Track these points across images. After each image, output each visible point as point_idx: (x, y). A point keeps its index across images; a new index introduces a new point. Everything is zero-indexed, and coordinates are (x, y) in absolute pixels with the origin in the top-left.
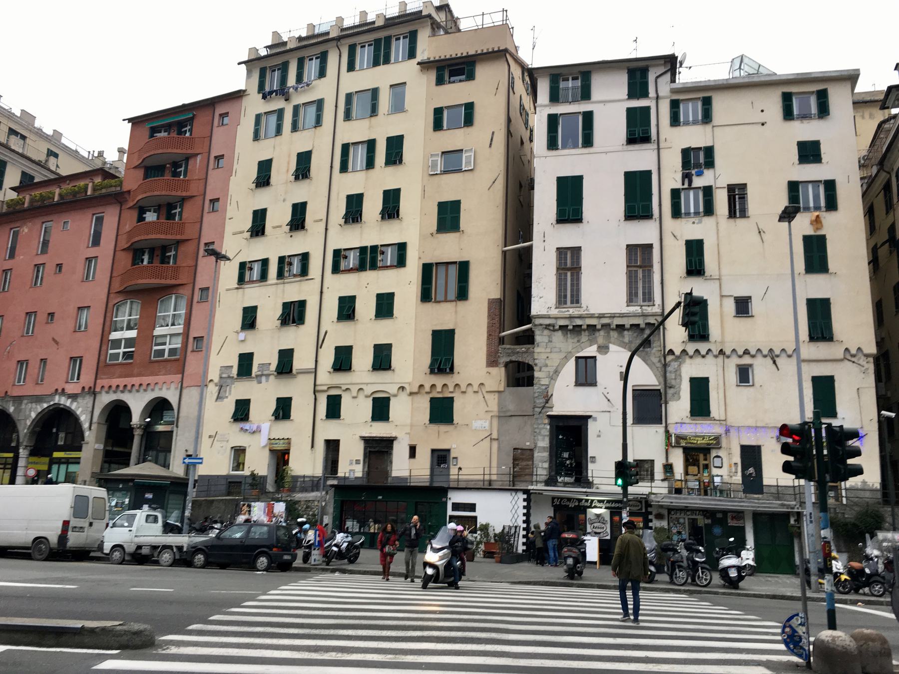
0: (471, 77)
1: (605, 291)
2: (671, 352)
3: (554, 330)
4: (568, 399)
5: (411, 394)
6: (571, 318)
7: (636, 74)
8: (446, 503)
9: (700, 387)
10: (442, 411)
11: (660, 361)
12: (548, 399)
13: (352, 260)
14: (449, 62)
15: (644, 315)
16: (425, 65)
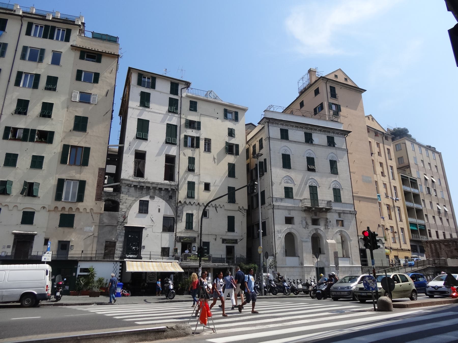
0: (99, 61)
1: (155, 172)
2: (180, 202)
3: (131, 187)
4: (134, 220)
5: (49, 211)
6: (139, 182)
7: (175, 86)
8: (77, 268)
9: (190, 217)
10: (67, 221)
11: (175, 205)
12: (125, 218)
13: (20, 134)
14: (87, 51)
15: (171, 185)
16: (73, 47)
